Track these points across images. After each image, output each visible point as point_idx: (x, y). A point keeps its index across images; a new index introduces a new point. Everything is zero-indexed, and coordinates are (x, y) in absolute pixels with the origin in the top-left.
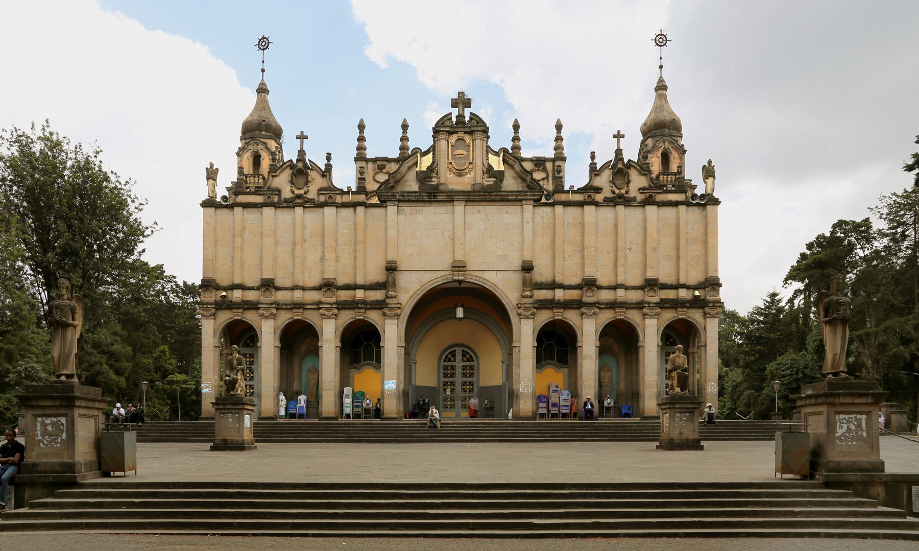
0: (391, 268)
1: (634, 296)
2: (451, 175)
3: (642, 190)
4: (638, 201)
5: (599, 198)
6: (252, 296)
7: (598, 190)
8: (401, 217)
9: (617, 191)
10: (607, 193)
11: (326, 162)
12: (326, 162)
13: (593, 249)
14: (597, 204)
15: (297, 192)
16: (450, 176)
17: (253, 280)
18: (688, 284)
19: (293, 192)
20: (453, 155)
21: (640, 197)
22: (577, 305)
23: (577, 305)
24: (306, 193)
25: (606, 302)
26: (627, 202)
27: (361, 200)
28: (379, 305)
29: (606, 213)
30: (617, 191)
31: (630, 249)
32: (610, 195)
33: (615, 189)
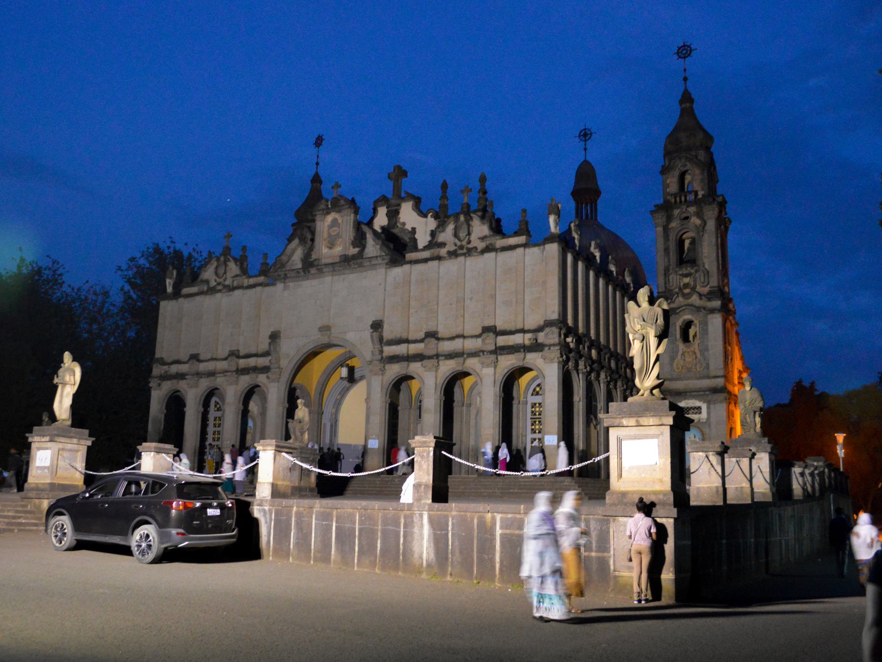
0: (274, 337)
1: (476, 344)
2: (326, 250)
3: (483, 239)
4: (479, 250)
5: (443, 252)
6: (184, 368)
7: (443, 245)
8: (286, 293)
9: (459, 243)
10: (450, 247)
11: (241, 253)
12: (241, 253)
13: (435, 303)
14: (439, 258)
15: (219, 280)
16: (325, 250)
17: (184, 355)
18: (526, 328)
19: (216, 281)
20: (329, 233)
21: (481, 245)
22: (419, 357)
23: (419, 357)
24: (225, 280)
25: (447, 353)
26: (470, 252)
27: (261, 281)
28: (265, 370)
29: (450, 267)
30: (459, 243)
31: (471, 299)
32: (453, 248)
33: (456, 241)
